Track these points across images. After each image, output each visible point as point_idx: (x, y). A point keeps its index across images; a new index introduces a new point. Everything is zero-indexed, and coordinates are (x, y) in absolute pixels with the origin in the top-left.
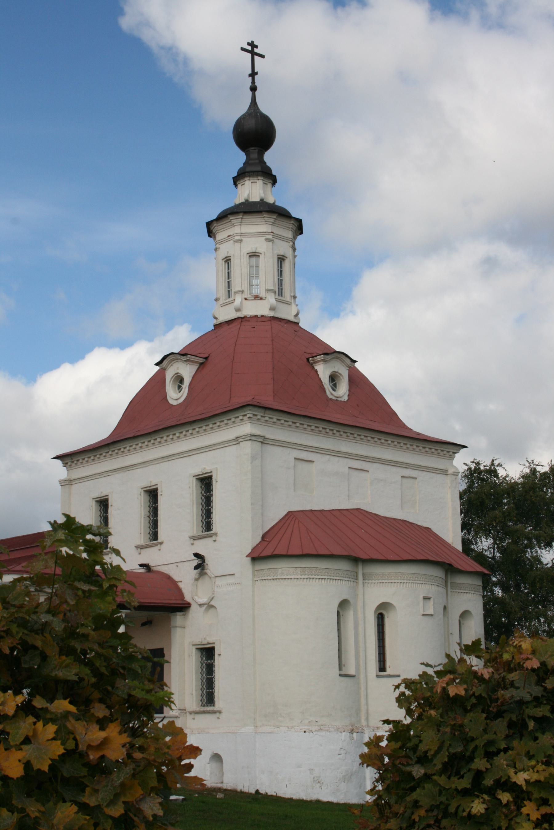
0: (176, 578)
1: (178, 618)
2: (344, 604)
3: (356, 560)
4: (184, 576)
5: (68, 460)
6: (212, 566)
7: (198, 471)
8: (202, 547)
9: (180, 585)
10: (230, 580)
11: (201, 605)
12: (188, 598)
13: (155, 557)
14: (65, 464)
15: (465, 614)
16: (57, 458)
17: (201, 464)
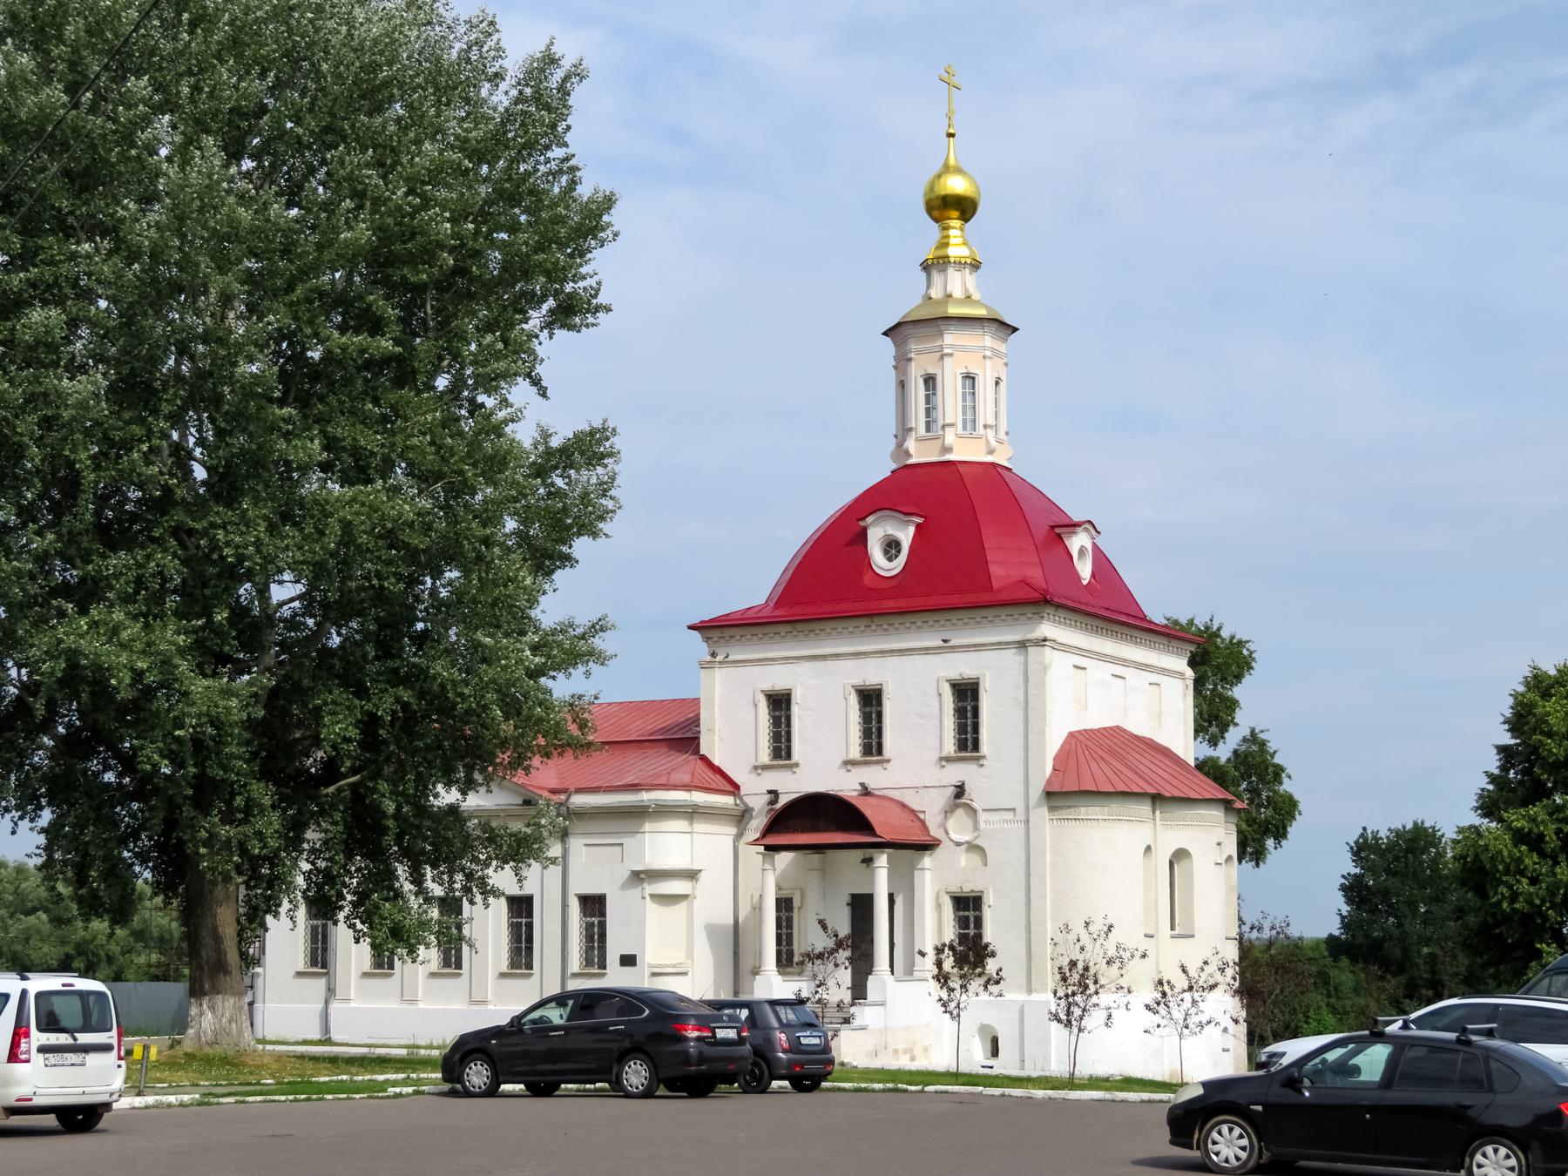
0: (915, 807)
1: (927, 861)
2: (1148, 848)
3: (1157, 799)
4: (931, 806)
5: (715, 634)
6: (975, 795)
7: (954, 675)
8: (961, 772)
9: (922, 816)
10: (1009, 815)
11: (958, 844)
12: (935, 832)
13: (874, 777)
14: (707, 639)
15: (1180, 855)
16: (690, 627)
17: (963, 666)
